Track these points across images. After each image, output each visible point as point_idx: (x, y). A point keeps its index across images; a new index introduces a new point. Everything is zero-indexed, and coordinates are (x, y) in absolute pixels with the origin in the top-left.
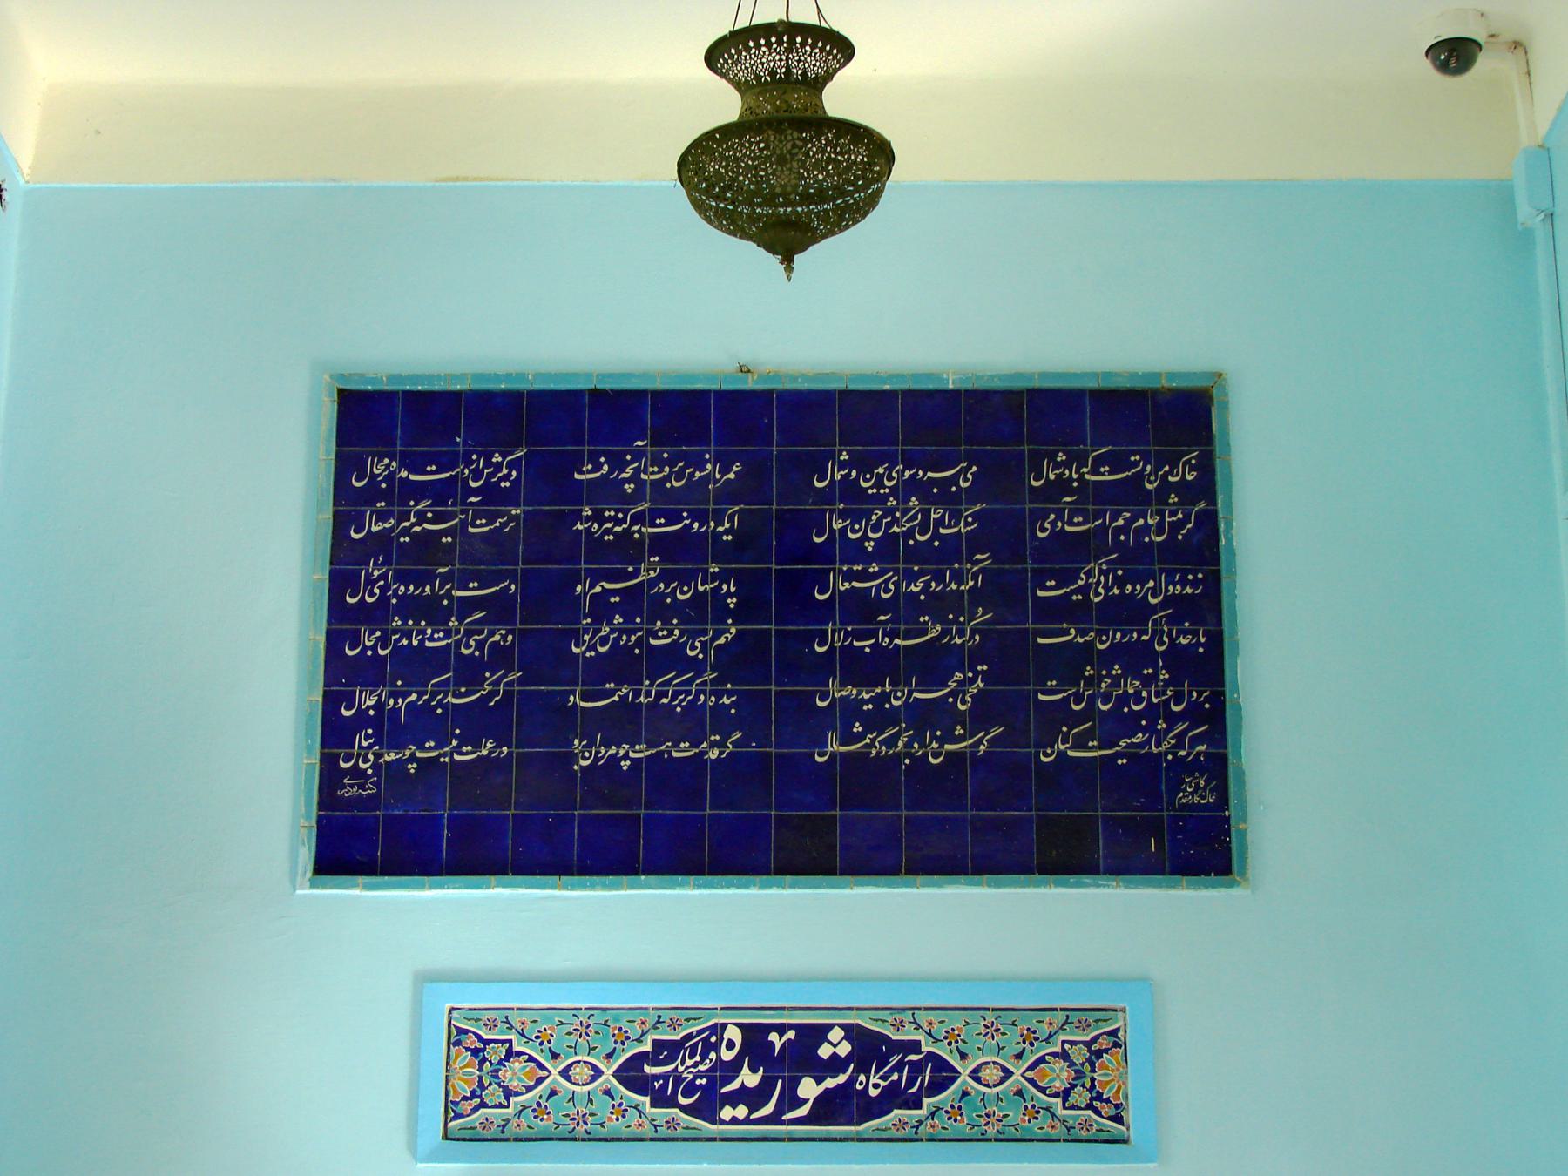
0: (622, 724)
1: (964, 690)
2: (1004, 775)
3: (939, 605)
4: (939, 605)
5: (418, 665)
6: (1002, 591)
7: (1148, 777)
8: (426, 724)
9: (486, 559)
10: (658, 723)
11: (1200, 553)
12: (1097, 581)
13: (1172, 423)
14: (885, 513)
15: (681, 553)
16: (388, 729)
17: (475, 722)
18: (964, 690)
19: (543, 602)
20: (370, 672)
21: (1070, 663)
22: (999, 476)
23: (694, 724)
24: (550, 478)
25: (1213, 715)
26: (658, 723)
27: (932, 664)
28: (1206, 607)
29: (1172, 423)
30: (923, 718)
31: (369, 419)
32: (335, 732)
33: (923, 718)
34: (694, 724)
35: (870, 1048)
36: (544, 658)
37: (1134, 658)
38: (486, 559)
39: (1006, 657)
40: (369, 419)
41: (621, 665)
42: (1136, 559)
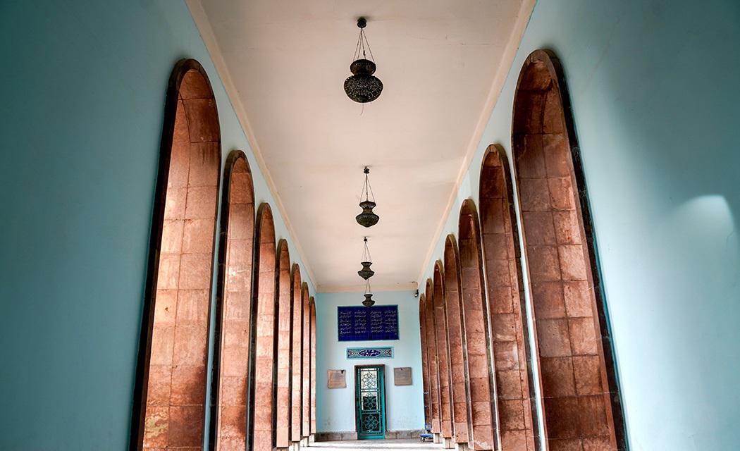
0: (359, 330)
1: (381, 327)
2: (384, 333)
3: (379, 322)
4: (379, 322)
5: (345, 327)
6: (383, 321)
7: (393, 333)
8: (346, 331)
9: (348, 319)
10: (361, 330)
11: (396, 317)
12: (389, 320)
13: (394, 308)
14: (375, 315)
15: (362, 319)
16: (343, 331)
17: (349, 330)
18: (381, 327)
19: (353, 323)
20: (342, 327)
21: (387, 325)
22: (383, 313)
23: (363, 330)
24: (353, 314)
25: (397, 329)
26: (361, 330)
27: (378, 326)
28: (397, 321)
29: (394, 308)
30: (378, 329)
31: (340, 309)
32: (339, 332)
33: (378, 329)
34: (363, 330)
35: (375, 351)
36: (353, 326)
37: (392, 325)
38: (348, 319)
39: (384, 325)
40: (340, 309)
41: (359, 326)
42: (392, 318)
